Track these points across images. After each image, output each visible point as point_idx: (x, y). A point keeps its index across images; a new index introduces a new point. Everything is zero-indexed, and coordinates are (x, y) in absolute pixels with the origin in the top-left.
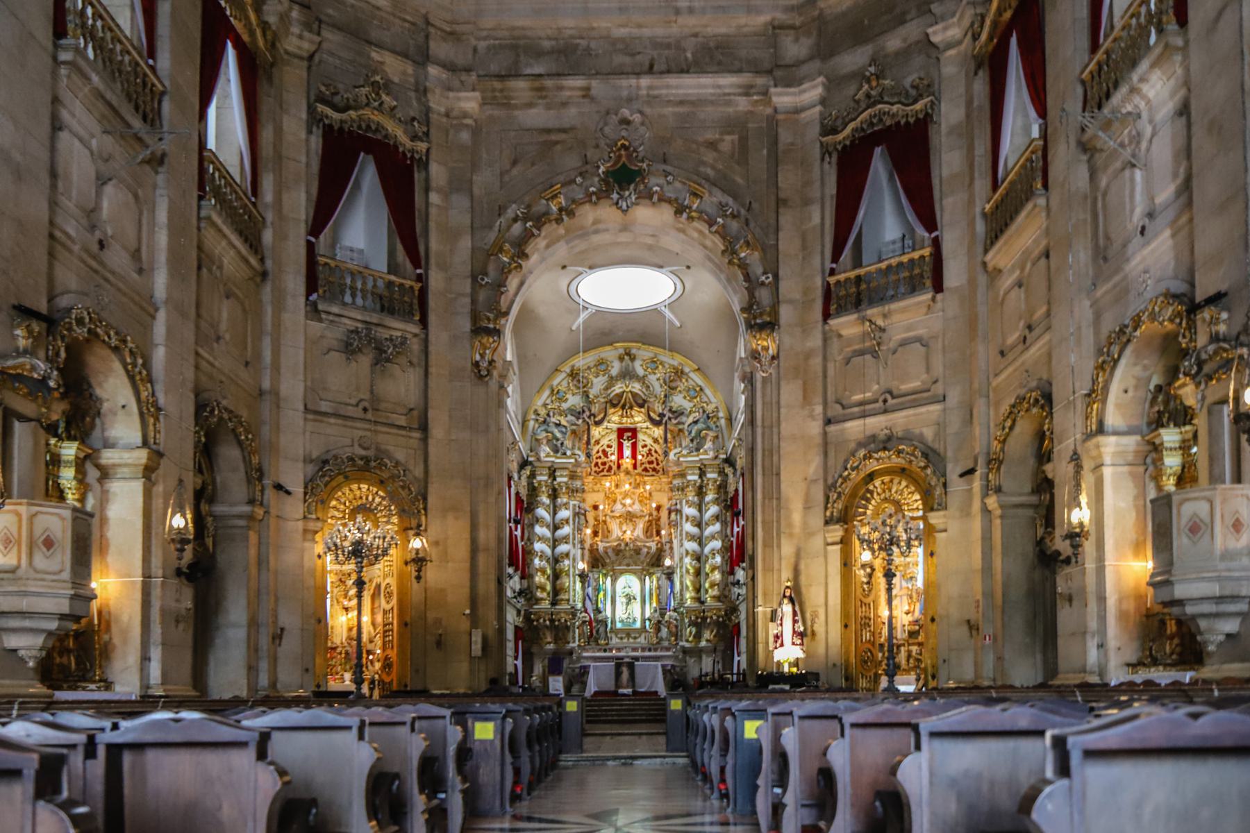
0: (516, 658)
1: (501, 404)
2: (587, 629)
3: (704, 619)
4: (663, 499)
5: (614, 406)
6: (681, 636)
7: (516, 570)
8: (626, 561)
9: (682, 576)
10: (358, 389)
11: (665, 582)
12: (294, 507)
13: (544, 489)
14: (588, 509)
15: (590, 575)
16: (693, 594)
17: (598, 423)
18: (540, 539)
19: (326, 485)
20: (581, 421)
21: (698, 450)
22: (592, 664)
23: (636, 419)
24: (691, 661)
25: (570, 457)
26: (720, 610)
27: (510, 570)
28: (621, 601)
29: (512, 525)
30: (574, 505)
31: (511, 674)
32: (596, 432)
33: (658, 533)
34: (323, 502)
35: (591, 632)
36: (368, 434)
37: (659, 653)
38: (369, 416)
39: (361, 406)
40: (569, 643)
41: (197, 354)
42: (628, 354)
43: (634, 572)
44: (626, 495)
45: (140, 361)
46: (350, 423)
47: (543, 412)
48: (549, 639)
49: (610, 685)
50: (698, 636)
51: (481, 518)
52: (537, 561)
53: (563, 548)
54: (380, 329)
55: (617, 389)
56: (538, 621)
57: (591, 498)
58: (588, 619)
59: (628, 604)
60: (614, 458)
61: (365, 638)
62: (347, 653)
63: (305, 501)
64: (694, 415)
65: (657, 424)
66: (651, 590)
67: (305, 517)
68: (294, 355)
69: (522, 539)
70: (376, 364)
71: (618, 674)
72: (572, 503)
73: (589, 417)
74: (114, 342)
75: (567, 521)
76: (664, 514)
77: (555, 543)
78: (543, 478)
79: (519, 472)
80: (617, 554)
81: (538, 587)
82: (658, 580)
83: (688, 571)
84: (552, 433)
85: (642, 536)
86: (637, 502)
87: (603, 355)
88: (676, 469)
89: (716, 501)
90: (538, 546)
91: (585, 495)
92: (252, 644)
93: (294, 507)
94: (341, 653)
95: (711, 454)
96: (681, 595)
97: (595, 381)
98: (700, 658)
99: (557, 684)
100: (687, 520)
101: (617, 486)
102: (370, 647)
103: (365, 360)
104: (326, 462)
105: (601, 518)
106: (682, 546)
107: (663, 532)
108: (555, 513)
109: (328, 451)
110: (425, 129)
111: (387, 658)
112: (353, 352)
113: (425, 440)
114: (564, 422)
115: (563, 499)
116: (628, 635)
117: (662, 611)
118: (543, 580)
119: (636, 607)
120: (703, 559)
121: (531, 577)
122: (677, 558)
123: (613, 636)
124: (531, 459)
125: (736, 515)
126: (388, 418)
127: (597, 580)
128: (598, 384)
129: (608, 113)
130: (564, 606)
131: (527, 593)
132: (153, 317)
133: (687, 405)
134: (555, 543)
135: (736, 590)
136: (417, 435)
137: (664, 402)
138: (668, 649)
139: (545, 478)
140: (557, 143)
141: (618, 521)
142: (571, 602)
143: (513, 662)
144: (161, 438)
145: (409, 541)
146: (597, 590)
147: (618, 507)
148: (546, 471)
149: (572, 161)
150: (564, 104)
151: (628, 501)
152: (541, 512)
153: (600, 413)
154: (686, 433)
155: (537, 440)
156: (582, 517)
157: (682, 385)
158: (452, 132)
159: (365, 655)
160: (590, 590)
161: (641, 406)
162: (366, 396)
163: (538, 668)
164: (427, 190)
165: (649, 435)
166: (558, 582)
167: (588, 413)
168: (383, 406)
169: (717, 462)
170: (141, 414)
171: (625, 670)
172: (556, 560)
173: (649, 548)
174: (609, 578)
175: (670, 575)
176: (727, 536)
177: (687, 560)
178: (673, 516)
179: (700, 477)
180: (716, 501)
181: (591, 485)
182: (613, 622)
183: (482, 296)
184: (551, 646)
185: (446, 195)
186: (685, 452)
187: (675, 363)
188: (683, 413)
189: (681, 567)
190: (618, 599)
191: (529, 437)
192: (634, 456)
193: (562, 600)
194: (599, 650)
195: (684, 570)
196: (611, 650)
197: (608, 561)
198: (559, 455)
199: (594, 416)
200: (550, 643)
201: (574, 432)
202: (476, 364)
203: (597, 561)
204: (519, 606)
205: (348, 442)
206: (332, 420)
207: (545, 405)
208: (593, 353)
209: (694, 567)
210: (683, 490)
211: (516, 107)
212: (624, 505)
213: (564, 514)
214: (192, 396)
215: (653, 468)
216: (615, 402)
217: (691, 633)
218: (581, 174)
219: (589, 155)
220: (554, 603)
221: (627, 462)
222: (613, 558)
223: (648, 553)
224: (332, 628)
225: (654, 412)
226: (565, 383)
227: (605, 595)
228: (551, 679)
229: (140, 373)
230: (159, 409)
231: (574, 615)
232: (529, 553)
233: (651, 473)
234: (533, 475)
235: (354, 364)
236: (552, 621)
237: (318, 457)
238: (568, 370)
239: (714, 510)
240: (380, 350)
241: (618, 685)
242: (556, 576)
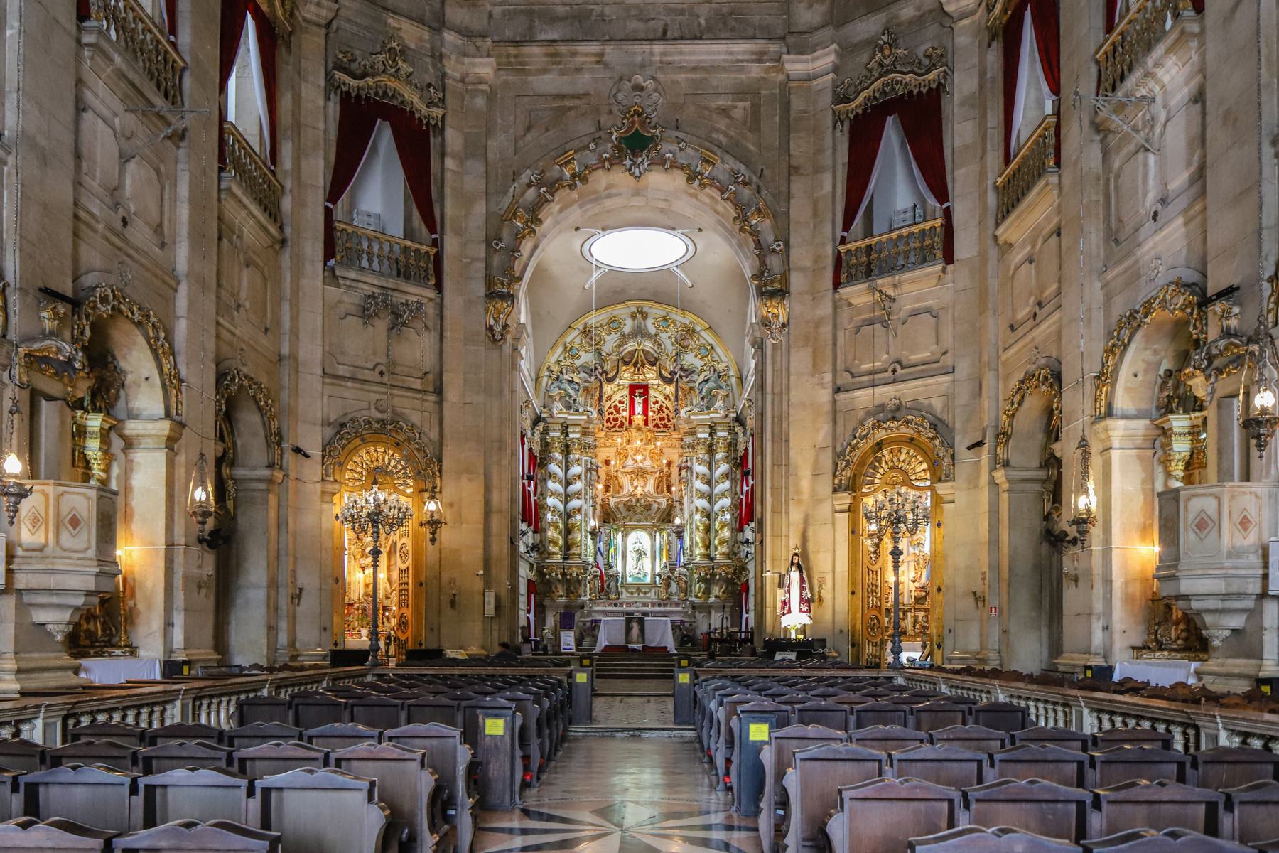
0: (529, 612)
1: (515, 367)
2: (597, 583)
3: (713, 575)
4: (673, 454)
5: (626, 363)
6: (691, 591)
7: (529, 526)
8: (637, 517)
9: (692, 533)
10: (374, 354)
11: (674, 537)
13: (556, 445)
14: (600, 465)
15: (602, 530)
16: (703, 551)
17: (610, 381)
18: (552, 494)
19: (343, 449)
20: (593, 378)
21: (708, 408)
22: (603, 619)
23: (648, 376)
24: (699, 616)
25: (582, 414)
26: (728, 566)
27: (523, 527)
28: (631, 557)
29: (526, 481)
30: (587, 461)
31: (523, 628)
32: (608, 389)
33: (669, 490)
34: (340, 464)
35: (602, 586)
36: (385, 397)
37: (668, 609)
38: (385, 379)
39: (378, 370)
40: (580, 596)
42: (640, 312)
43: (644, 528)
44: (637, 451)
46: (366, 387)
47: (556, 369)
48: (561, 593)
49: (620, 640)
50: (707, 592)
51: (495, 480)
52: (549, 516)
53: (575, 503)
54: (395, 294)
55: (630, 347)
56: (550, 574)
57: (603, 454)
58: (599, 573)
59: (638, 559)
60: (626, 414)
61: (381, 594)
62: (364, 609)
64: (705, 373)
65: (668, 381)
66: (661, 545)
67: (323, 480)
68: (312, 319)
69: (535, 495)
70: (392, 328)
71: (628, 630)
72: (584, 458)
73: (602, 375)
75: (579, 476)
76: (674, 470)
77: (567, 498)
78: (555, 434)
79: (532, 429)
80: (629, 510)
81: (550, 542)
82: (668, 535)
83: (697, 528)
84: (565, 390)
85: (652, 492)
86: (648, 458)
87: (615, 313)
88: (686, 426)
89: (726, 459)
90: (551, 501)
91: (596, 451)
93: (312, 470)
94: (358, 609)
95: (722, 413)
96: (691, 551)
97: (607, 338)
98: (710, 613)
99: (568, 639)
100: (697, 477)
101: (628, 442)
102: (386, 603)
103: (382, 325)
104: (343, 425)
105: (612, 473)
106: (692, 502)
107: (673, 489)
108: (567, 469)
109: (346, 414)
110: (441, 95)
111: (402, 616)
112: (370, 317)
113: (440, 403)
114: (576, 380)
115: (574, 456)
116: (639, 590)
117: (672, 566)
118: (555, 535)
119: (646, 563)
120: (713, 516)
121: (544, 531)
122: (687, 515)
123: (624, 590)
124: (543, 415)
125: (745, 474)
126: (403, 381)
127: (608, 535)
128: (610, 342)
129: (621, 79)
130: (576, 560)
131: (539, 548)
133: (698, 363)
134: (567, 498)
135: (745, 549)
136: (432, 398)
137: (675, 361)
138: (677, 605)
139: (558, 434)
140: (571, 108)
141: (629, 476)
142: (583, 557)
143: (525, 616)
145: (425, 503)
146: (609, 545)
147: (630, 462)
148: (558, 427)
149: (586, 127)
150: (578, 70)
151: (639, 458)
152: (554, 468)
153: (612, 370)
154: (698, 392)
155: (550, 396)
156: (594, 473)
157: (693, 344)
158: (467, 97)
159: (381, 611)
160: (601, 545)
161: (653, 364)
162: (383, 360)
163: (550, 621)
164: (443, 155)
165: (660, 393)
166: (570, 537)
167: (600, 371)
168: (399, 369)
169: (728, 420)
171: (635, 625)
172: (569, 515)
173: (660, 504)
174: (620, 534)
175: (679, 534)
176: (736, 494)
177: (697, 517)
178: (683, 472)
179: (711, 435)
180: (726, 459)
181: (602, 441)
182: (624, 577)
183: (496, 260)
184: (563, 600)
185: (462, 159)
186: (695, 410)
187: (687, 322)
188: (693, 372)
189: (691, 524)
190: (628, 553)
191: (542, 394)
192: (645, 413)
193: (574, 554)
194: (610, 605)
195: (694, 526)
196: (621, 604)
197: (619, 516)
198: (571, 411)
199: (607, 373)
200: (561, 596)
201: (586, 389)
202: (491, 329)
203: (608, 517)
204: (531, 560)
205: (365, 405)
206: (349, 384)
207: (558, 362)
208: (606, 310)
209: (703, 524)
210: (693, 447)
211: (529, 73)
212: (635, 461)
213: (576, 470)
215: (664, 425)
216: (627, 360)
217: (700, 589)
218: (594, 140)
219: (602, 122)
220: (565, 558)
221: (639, 419)
222: (625, 513)
223: (659, 509)
224: (350, 584)
225: (666, 370)
226: (577, 341)
227: (616, 550)
228: (562, 633)
231: (585, 569)
232: (541, 507)
233: (662, 429)
234: (546, 431)
235: (370, 329)
236: (564, 575)
237: (336, 420)
238: (581, 327)
239: (724, 468)
241: (628, 641)
242: (568, 531)
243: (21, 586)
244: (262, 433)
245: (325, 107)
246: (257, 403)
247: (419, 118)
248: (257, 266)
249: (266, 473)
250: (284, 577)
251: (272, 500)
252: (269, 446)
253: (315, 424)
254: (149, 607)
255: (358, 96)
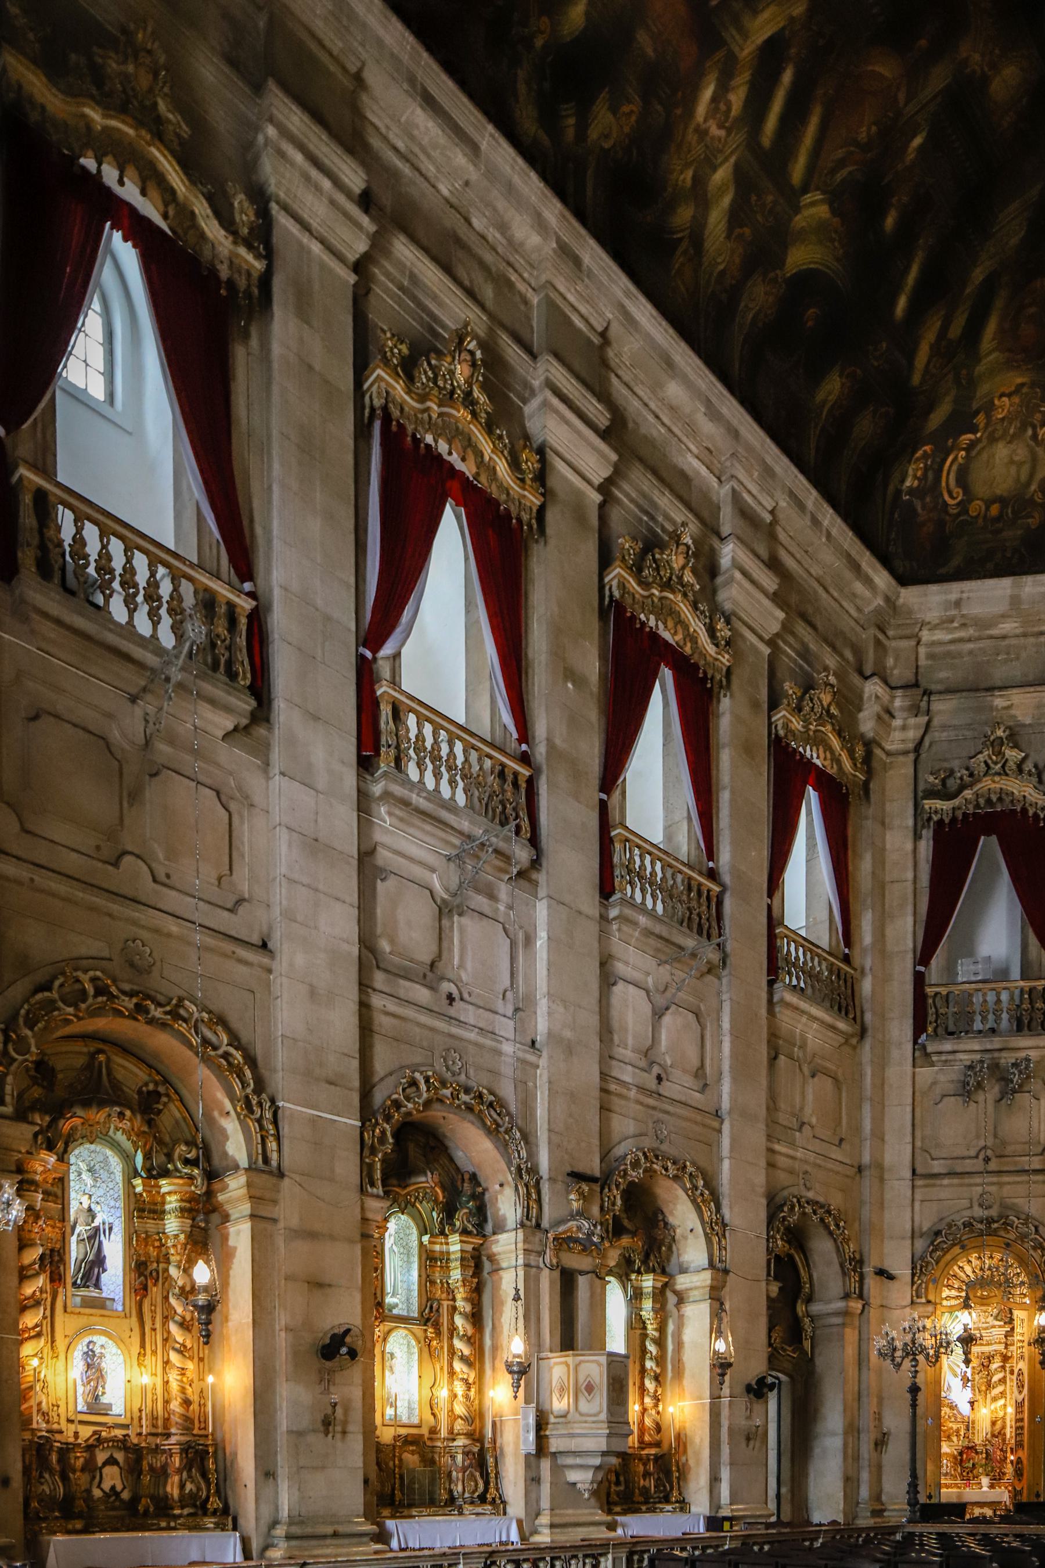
10: (978, 1137)
12: (901, 1292)
19: (937, 1263)
34: (935, 1281)
36: (993, 1189)
38: (993, 1166)
39: (982, 1156)
41: (771, 1151)
45: (701, 1183)
46: (967, 1181)
54: (1004, 1054)
63: (913, 1283)
67: (912, 1302)
70: (1001, 1099)
74: (672, 1172)
92: (850, 1451)
93: (901, 1292)
104: (938, 1233)
109: (942, 1219)
132: (720, 1131)
144: (728, 1256)
168: (1010, 1150)
170: (706, 1234)
205: (965, 1203)
206: (946, 1182)
214: (764, 1201)
229: (702, 1195)
230: (725, 1225)
235: (973, 1105)
237: (930, 1229)
240: (1005, 1080)
243: (553, 1450)
244: (836, 1261)
245: (915, 850)
246: (827, 1227)
247: (1036, 815)
248: (827, 1073)
249: (840, 1305)
250: (867, 1422)
251: (851, 1335)
252: (844, 1274)
253: (903, 1238)
254: (698, 1462)
255: (954, 819)
